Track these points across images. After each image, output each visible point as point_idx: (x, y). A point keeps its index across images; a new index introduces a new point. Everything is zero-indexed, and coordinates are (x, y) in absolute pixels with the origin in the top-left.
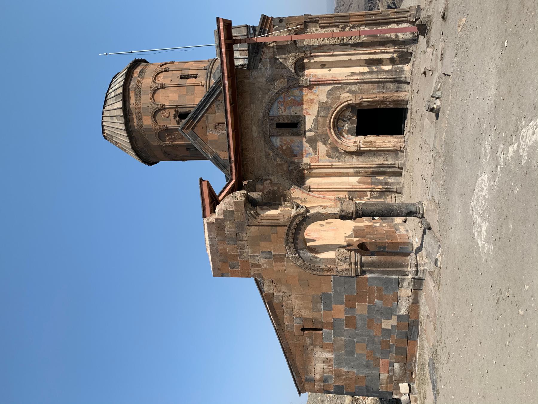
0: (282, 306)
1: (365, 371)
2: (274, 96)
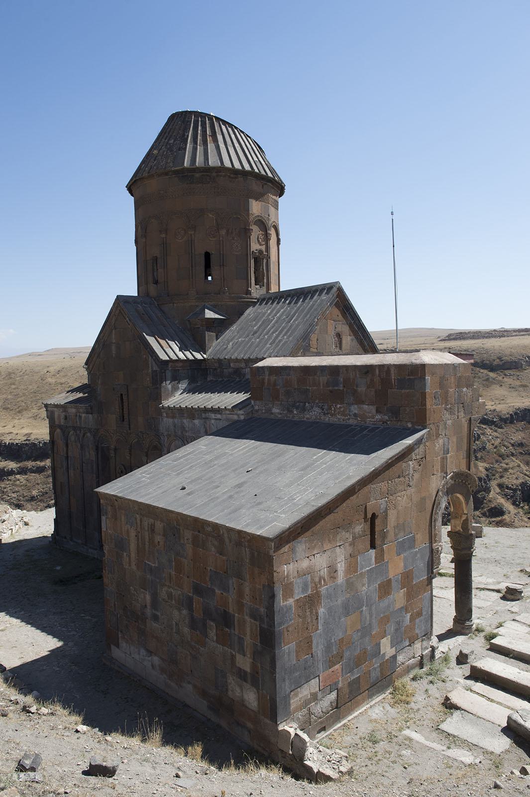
0: (399, 477)
1: (321, 647)
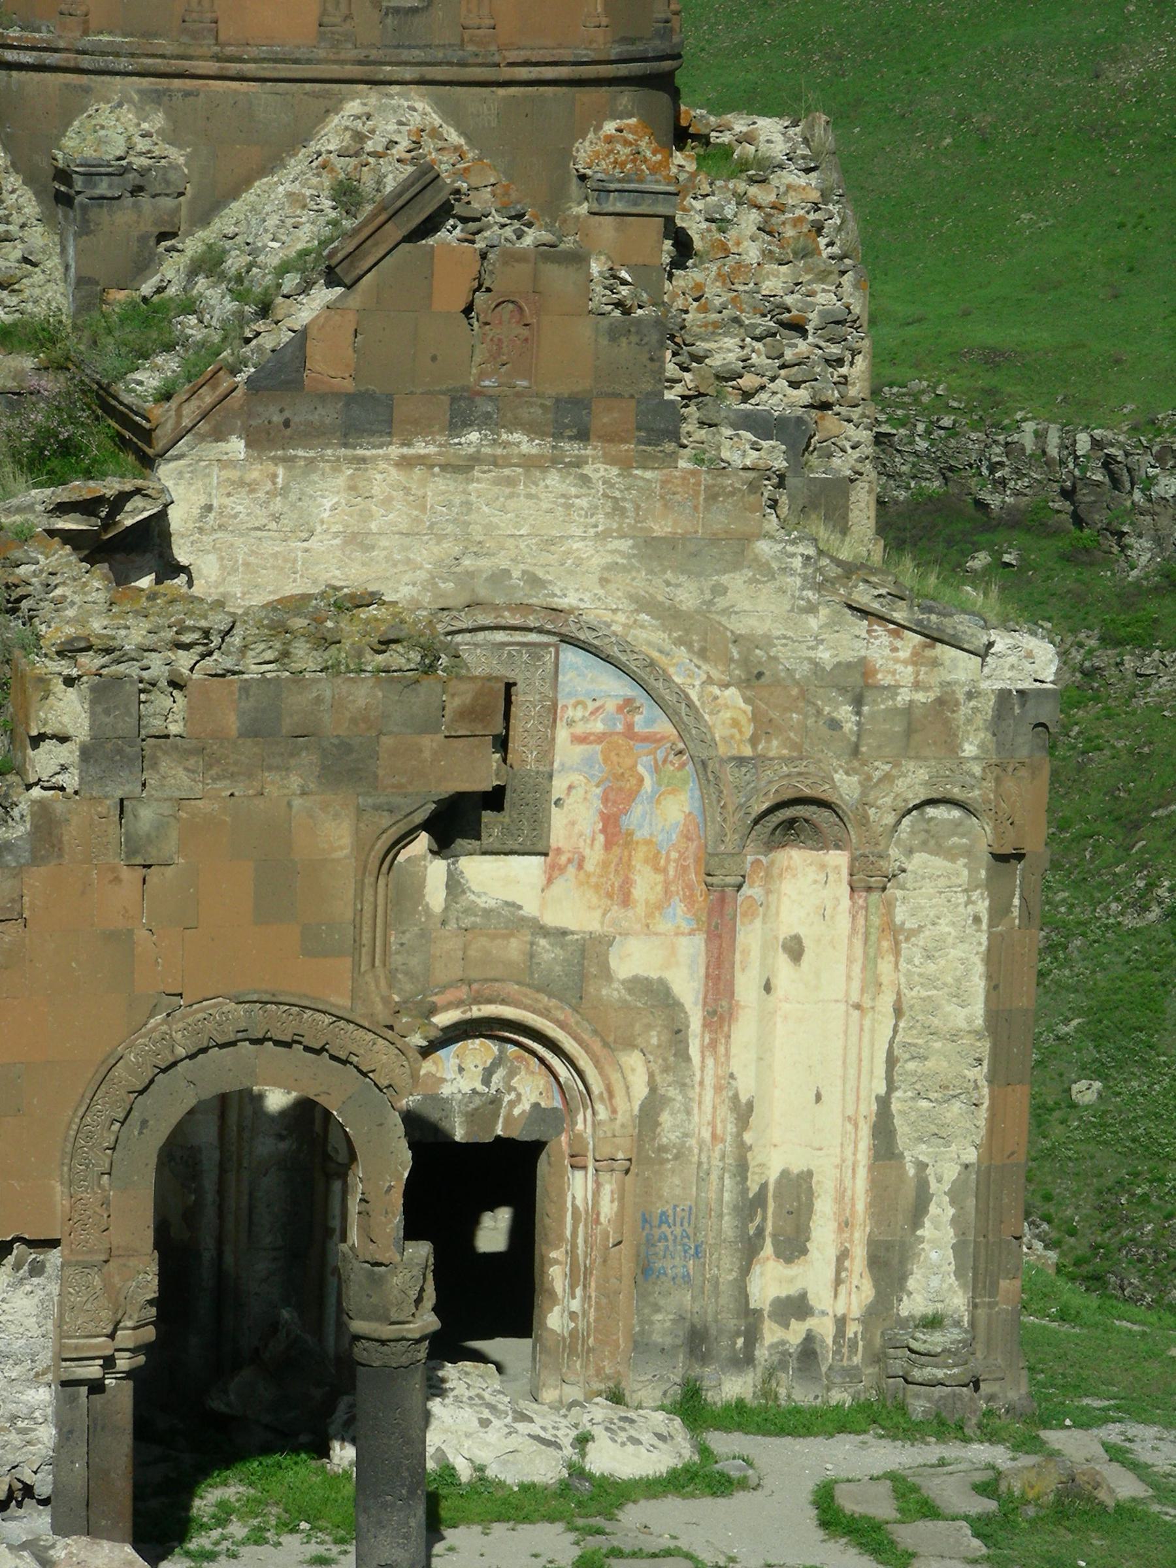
2: (668, 679)
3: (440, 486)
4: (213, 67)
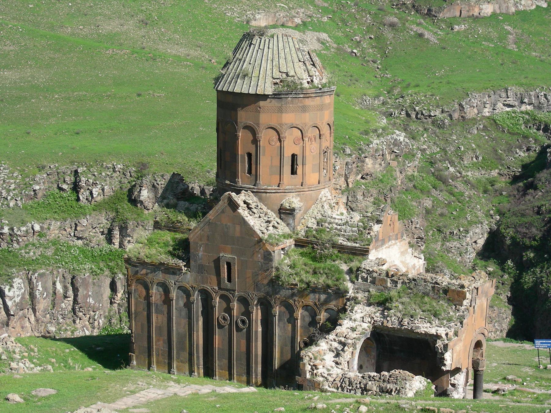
3: (388, 250)
4: (308, 190)
